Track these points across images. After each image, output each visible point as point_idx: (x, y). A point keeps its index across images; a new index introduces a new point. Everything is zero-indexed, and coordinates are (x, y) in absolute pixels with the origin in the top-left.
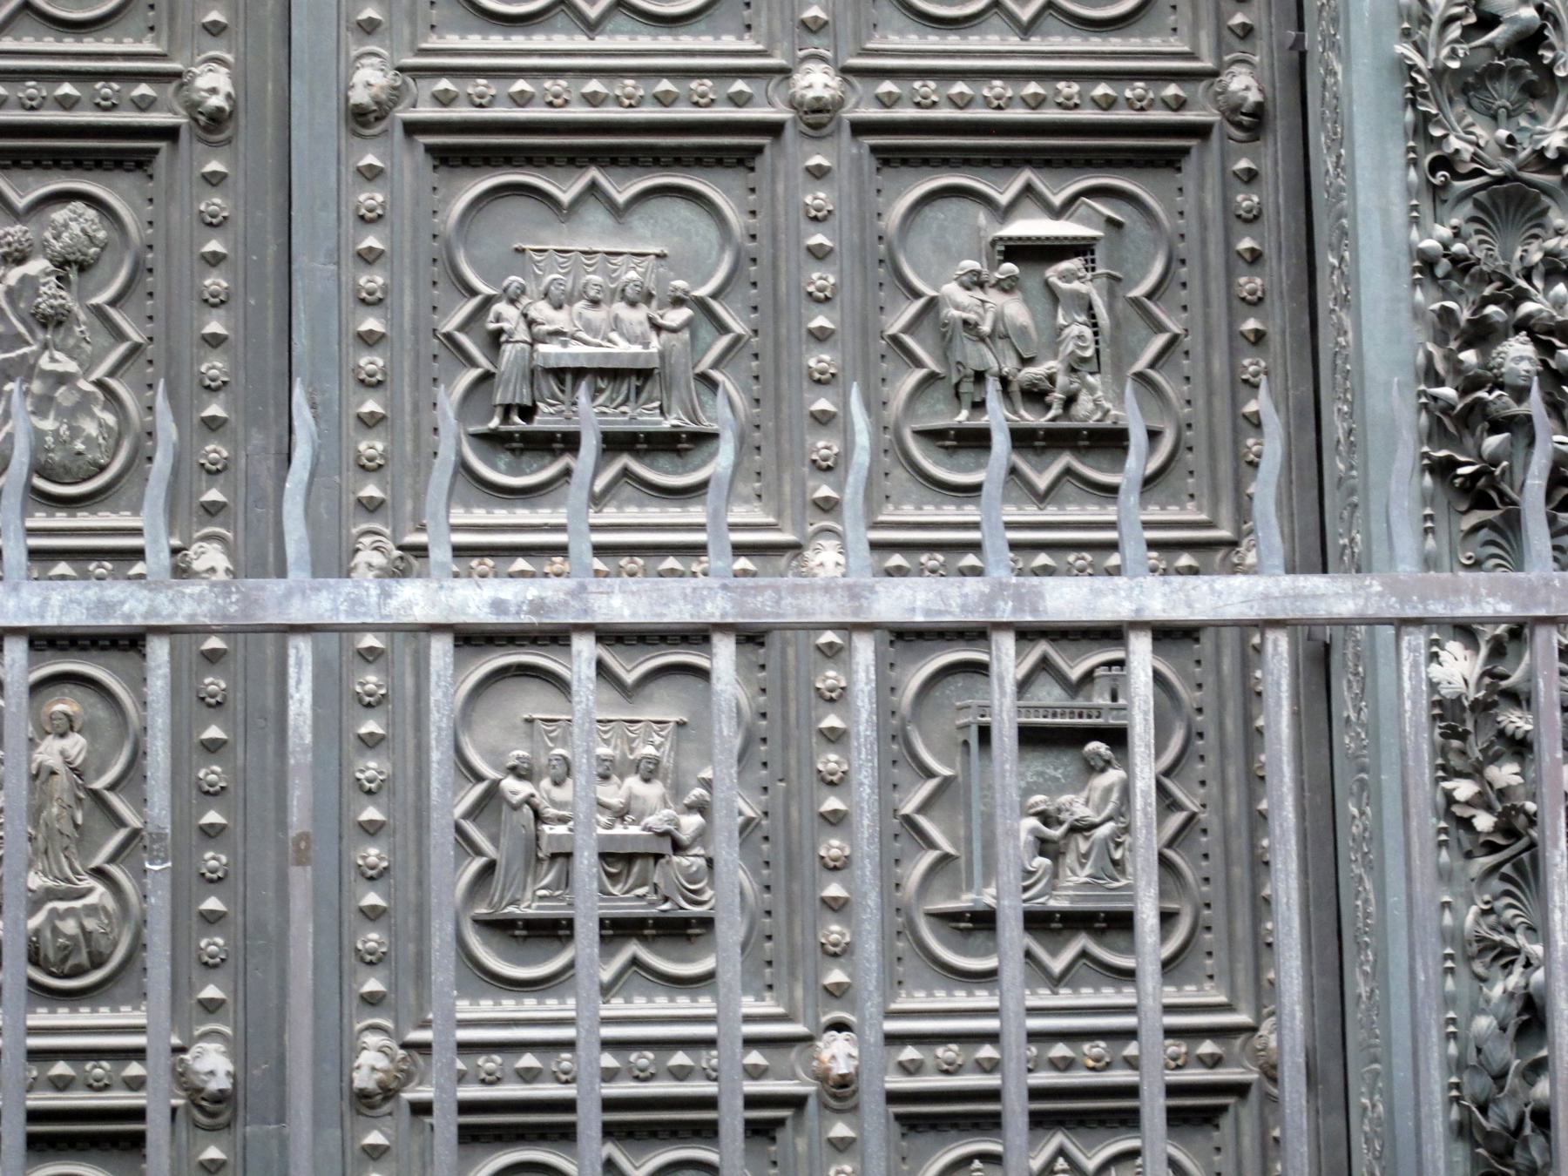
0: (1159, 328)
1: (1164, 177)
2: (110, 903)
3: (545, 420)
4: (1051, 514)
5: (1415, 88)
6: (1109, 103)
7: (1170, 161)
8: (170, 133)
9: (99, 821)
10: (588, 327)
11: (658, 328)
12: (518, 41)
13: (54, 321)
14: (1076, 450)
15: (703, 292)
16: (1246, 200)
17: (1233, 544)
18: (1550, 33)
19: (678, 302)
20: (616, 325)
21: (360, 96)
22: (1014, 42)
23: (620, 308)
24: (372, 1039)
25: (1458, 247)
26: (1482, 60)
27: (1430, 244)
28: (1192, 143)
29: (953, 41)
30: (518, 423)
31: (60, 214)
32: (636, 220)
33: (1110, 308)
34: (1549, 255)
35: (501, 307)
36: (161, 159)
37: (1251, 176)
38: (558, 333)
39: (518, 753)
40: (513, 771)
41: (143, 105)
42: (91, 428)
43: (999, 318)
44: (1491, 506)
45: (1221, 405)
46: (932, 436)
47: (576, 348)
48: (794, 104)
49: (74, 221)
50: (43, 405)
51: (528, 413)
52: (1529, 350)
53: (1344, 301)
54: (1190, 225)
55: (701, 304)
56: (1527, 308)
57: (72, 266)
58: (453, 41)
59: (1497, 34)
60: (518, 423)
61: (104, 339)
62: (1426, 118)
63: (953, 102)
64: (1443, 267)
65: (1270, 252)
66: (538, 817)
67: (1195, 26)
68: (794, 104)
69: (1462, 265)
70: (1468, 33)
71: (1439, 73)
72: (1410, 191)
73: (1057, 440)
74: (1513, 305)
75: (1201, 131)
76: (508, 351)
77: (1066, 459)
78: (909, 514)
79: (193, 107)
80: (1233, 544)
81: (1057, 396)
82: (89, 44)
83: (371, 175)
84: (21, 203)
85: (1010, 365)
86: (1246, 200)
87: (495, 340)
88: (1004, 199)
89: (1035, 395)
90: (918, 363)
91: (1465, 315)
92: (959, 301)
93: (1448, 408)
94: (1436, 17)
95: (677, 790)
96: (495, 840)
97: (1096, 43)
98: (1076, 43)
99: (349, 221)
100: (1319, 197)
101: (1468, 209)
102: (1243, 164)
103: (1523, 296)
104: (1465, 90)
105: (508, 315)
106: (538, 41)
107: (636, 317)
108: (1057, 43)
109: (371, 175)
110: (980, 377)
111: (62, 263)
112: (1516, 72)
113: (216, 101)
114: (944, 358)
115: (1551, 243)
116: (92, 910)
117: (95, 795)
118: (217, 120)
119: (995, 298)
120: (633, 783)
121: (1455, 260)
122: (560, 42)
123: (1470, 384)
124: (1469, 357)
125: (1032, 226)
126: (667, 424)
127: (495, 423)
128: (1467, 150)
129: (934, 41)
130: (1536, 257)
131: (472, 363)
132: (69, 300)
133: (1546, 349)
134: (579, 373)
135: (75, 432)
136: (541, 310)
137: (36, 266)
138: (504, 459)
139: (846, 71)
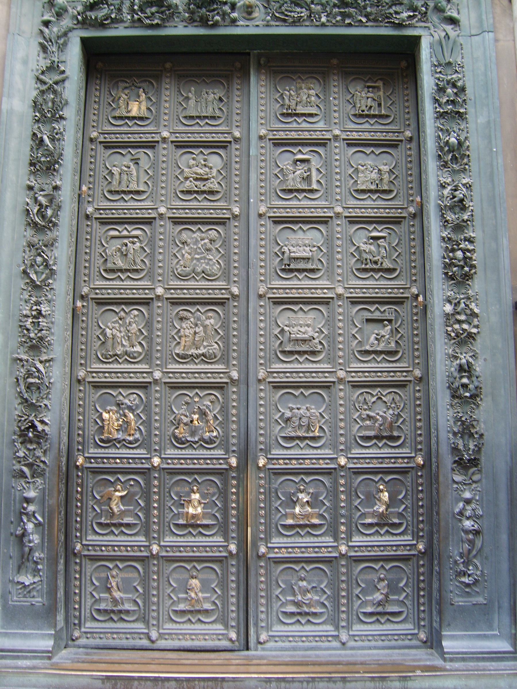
0: (397, 251)
1: (398, 226)
2: (218, 348)
3: (292, 266)
4: (378, 283)
5: (442, 209)
6: (389, 213)
7: (399, 223)
8: (229, 219)
9: (216, 334)
10: (299, 251)
11: (311, 251)
12: (288, 203)
13: (209, 250)
14: (383, 272)
15: (319, 245)
16: (412, 229)
17: (409, 288)
18: (465, 199)
19: (314, 246)
20: (304, 250)
21: (261, 212)
22: (372, 203)
23: (305, 248)
24: (261, 371)
25: (449, 236)
26: (453, 204)
27: (444, 235)
28: (403, 220)
29: (362, 203)
30: (287, 267)
31: (210, 232)
32: (308, 233)
33: (389, 247)
34: (465, 237)
35: (285, 247)
36: (228, 223)
37: (413, 225)
38: (294, 252)
39: (287, 323)
40: (286, 326)
41: (224, 214)
42: (215, 268)
43: (370, 249)
44: (454, 280)
45: (408, 264)
46: (358, 270)
47: (297, 254)
48: (334, 213)
49: (213, 233)
50: (207, 264)
51: (289, 265)
52: (461, 253)
53: (429, 246)
54: (403, 234)
55: (318, 247)
56: (461, 246)
57: (212, 241)
58: (277, 203)
59: (455, 199)
60: (287, 267)
61: (218, 253)
62: (443, 214)
63: (362, 213)
64: (446, 239)
65: (416, 238)
66: (290, 333)
67: (404, 200)
68: (334, 213)
69: (449, 239)
70: (451, 199)
71: (445, 206)
72: (440, 226)
73: (379, 270)
74: (458, 245)
75: (404, 218)
76: (286, 255)
77: (381, 273)
78: (354, 283)
79: (233, 214)
80: (409, 288)
81: (379, 263)
82: (215, 204)
83: (262, 225)
84: (204, 230)
85: (371, 258)
86: (412, 229)
87: (283, 253)
88: (370, 229)
89: (376, 263)
90: (355, 257)
91: (450, 247)
92: (363, 247)
93: (447, 263)
94: (445, 196)
95: (314, 329)
96: (283, 337)
97: (386, 203)
98: (383, 203)
99: (259, 233)
100: (425, 229)
101: (451, 229)
102: (412, 223)
103: (460, 244)
104: (450, 209)
105: (286, 249)
106: (291, 203)
107: (308, 249)
108: (380, 203)
109: (262, 225)
110: (366, 259)
111: (211, 240)
112: (459, 206)
113: (236, 213)
114: (360, 256)
115: (465, 235)
116: (215, 349)
117: (215, 329)
118: (237, 216)
119: (369, 246)
120: (306, 328)
121: (448, 238)
122: (295, 203)
123: (451, 259)
124: (451, 254)
125: (375, 234)
126: (312, 267)
127: (283, 267)
128: (451, 219)
129: (359, 202)
130: (463, 238)
131: (279, 257)
132: (211, 246)
133: (464, 253)
134: (297, 258)
135: (213, 268)
136: (291, 248)
137: (206, 241)
138: (285, 273)
139: (343, 208)
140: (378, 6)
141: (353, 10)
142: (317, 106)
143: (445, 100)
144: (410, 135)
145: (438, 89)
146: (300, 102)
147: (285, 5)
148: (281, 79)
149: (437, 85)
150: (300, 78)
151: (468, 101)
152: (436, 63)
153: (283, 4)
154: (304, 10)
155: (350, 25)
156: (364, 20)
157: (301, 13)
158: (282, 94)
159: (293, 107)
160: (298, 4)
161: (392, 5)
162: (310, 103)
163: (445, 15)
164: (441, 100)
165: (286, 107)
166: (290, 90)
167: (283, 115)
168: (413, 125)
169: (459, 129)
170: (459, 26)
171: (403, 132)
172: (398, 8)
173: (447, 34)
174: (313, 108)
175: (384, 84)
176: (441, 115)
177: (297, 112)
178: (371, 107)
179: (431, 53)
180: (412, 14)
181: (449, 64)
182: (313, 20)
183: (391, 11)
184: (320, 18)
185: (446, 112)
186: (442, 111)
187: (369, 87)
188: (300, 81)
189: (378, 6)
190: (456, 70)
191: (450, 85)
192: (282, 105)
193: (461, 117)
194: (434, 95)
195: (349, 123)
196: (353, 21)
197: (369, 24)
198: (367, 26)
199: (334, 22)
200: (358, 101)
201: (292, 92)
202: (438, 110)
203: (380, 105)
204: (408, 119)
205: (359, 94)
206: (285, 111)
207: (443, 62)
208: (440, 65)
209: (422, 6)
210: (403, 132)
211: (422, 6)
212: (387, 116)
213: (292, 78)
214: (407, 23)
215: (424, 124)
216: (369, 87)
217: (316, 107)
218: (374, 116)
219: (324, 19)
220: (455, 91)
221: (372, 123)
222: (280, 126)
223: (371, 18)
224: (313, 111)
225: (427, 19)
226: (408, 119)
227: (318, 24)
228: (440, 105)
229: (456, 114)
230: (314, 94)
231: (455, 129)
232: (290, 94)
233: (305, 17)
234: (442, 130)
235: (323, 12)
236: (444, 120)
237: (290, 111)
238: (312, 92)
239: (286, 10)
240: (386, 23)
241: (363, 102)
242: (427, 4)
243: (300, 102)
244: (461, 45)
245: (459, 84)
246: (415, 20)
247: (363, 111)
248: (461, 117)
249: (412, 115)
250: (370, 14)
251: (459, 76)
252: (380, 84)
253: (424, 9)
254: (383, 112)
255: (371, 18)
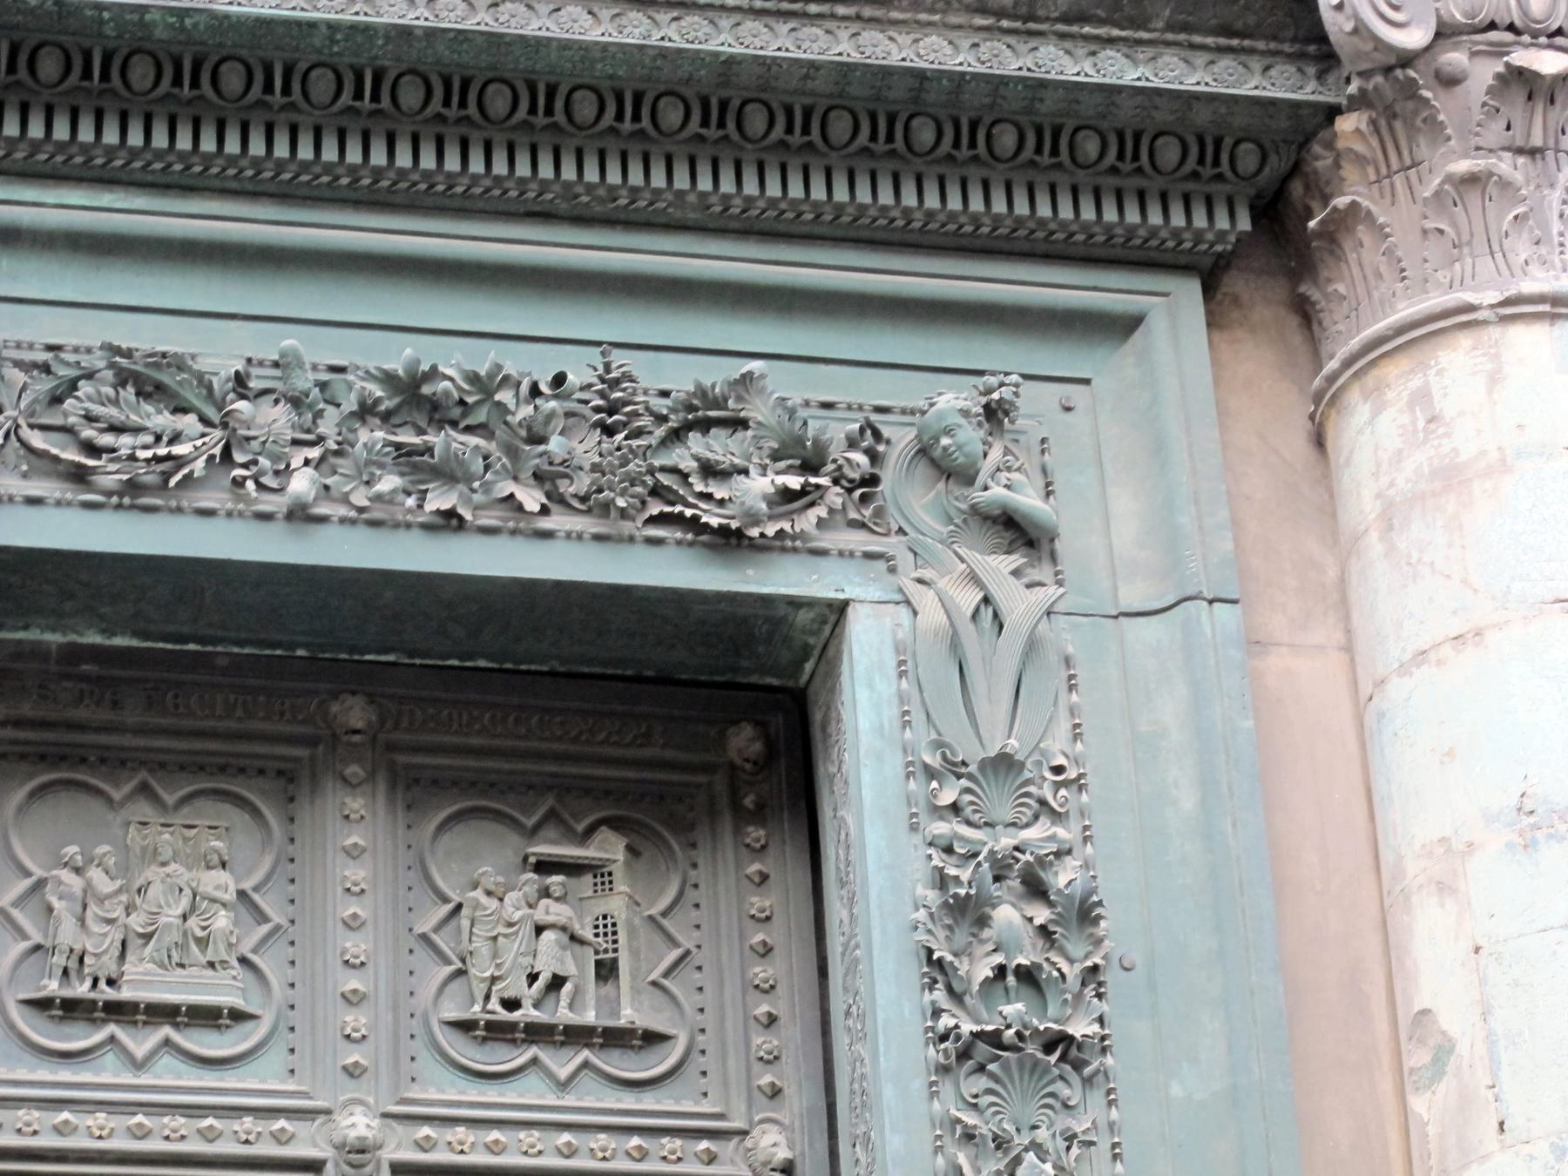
140: (609, 431)
141: (474, 440)
142: (243, 961)
143: (985, 971)
144: (783, 1154)
145: (945, 904)
146: (147, 937)
147: (85, 388)
148: (34, 795)
149: (942, 881)
150: (145, 790)
151: (1111, 977)
152: (933, 760)
153: (73, 385)
154: (189, 422)
155: (450, 521)
156: (531, 499)
157: (175, 439)
158: (40, 884)
159: (109, 966)
160: (159, 387)
161: (689, 426)
162: (203, 943)
163: (978, 496)
164: (963, 967)
165: (59, 960)
166: (89, 861)
167: (42, 1005)
168: (801, 1097)
169: (1070, 1138)
170: (1053, 557)
171: (744, 1133)
172: (719, 446)
173: (986, 600)
174: (222, 978)
175: (630, 849)
176: (964, 1055)
177: (126, 994)
178: (557, 982)
179: (902, 698)
180: (794, 482)
181: (1004, 764)
182: (239, 483)
183: (683, 457)
184: (285, 473)
185: (994, 1039)
186: (967, 1027)
187: (544, 867)
188: (144, 809)
189: (609, 431)
190: (1043, 802)
191: (1015, 883)
192: (38, 948)
193: (1078, 1066)
194: (921, 936)
195: (428, 1064)
196: (467, 501)
197: (558, 521)
198: (547, 535)
199: (360, 499)
200: (481, 946)
201: (95, 874)
202: (946, 1021)
203: (606, 971)
204: (771, 1060)
205: (493, 904)
206: (52, 987)
207: (971, 751)
208: (956, 768)
209: (852, 444)
210: (744, 1133)
211: (852, 444)
212: (652, 1039)
213: (98, 792)
214: (771, 530)
215: (865, 1101)
216: (544, 867)
217: (237, 970)
218: (576, 1036)
219: (302, 484)
220: (1042, 915)
221: (563, 1073)
222: (22, 1074)
223: (567, 488)
224: (222, 992)
225: (879, 513)
226: (771, 1060)
227: (269, 503)
228: (956, 996)
229: (1048, 1048)
230: (230, 896)
231: (1042, 1135)
232: (88, 888)
233: (199, 466)
234: (969, 1136)
235: (296, 443)
236: (983, 1082)
237: (82, 990)
238: (219, 883)
239: (90, 418)
240: (652, 520)
241: (512, 950)
242: (877, 435)
243: (147, 937)
244: (1067, 662)
245: (1062, 877)
246: (813, 514)
247: (511, 1004)
248: (1078, 1066)
249: (794, 1037)
250: (567, 468)
251: (1061, 832)
252: (609, 848)
253: (860, 458)
254: (629, 1015)
255: (567, 488)
